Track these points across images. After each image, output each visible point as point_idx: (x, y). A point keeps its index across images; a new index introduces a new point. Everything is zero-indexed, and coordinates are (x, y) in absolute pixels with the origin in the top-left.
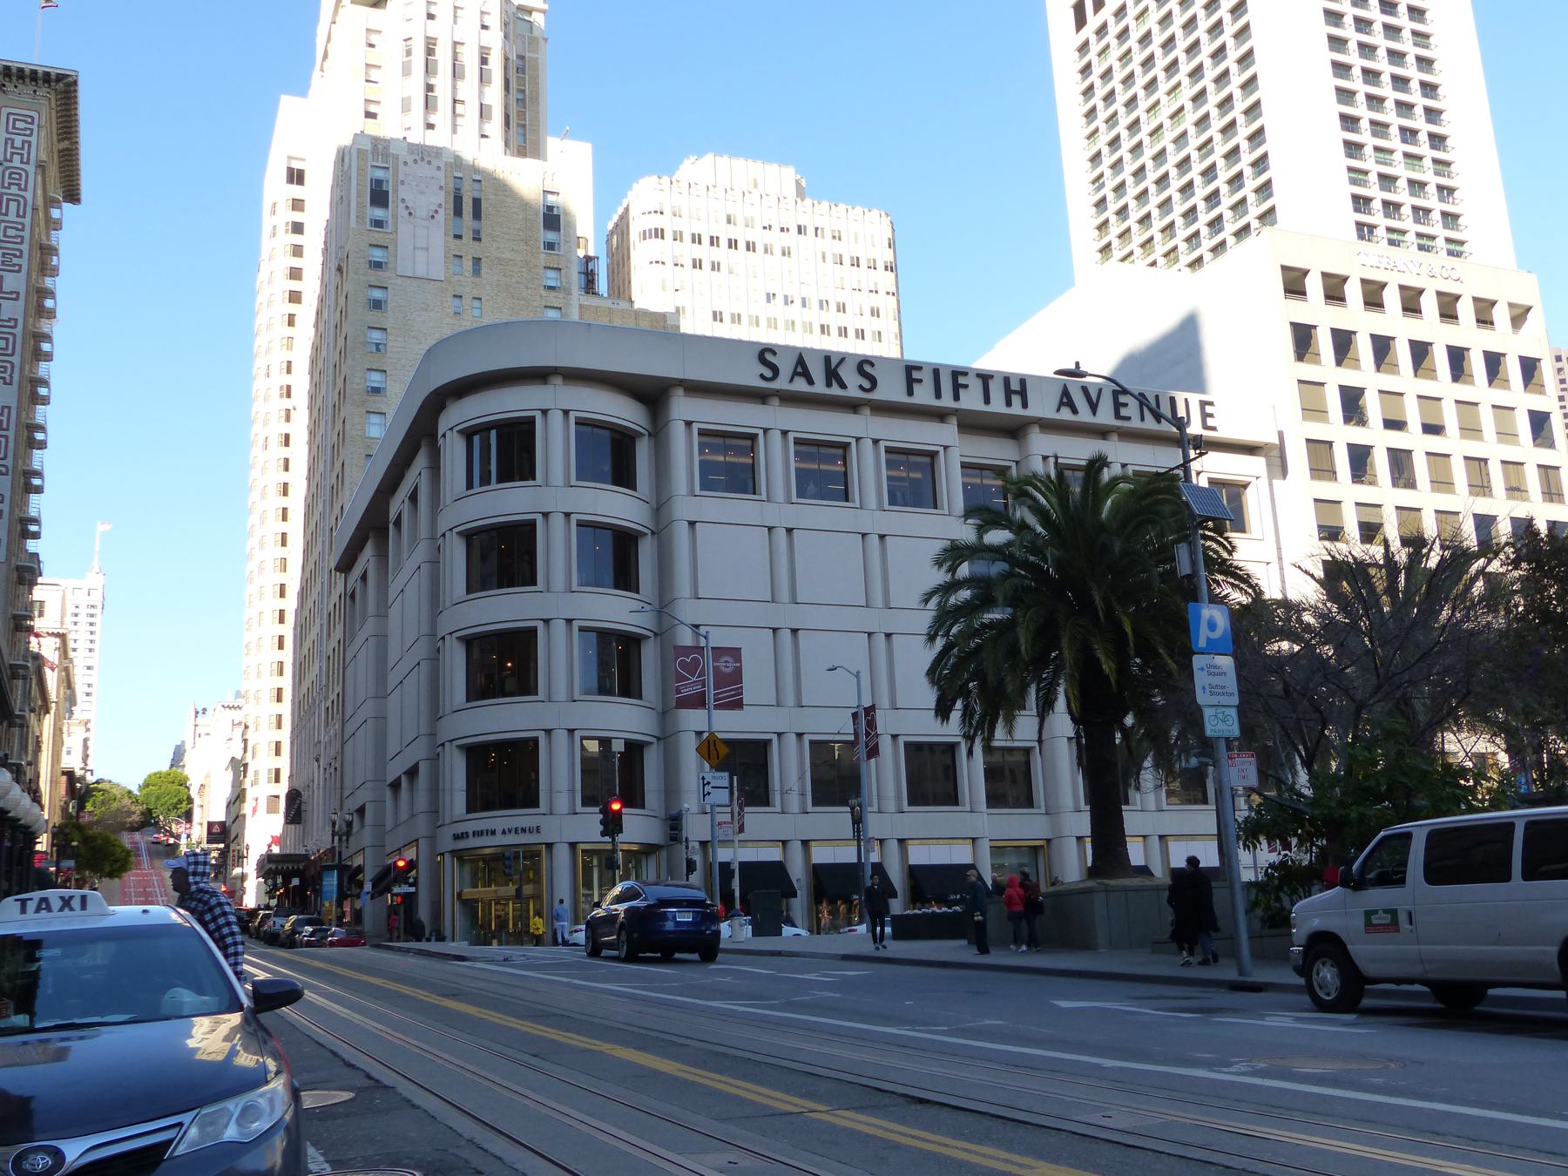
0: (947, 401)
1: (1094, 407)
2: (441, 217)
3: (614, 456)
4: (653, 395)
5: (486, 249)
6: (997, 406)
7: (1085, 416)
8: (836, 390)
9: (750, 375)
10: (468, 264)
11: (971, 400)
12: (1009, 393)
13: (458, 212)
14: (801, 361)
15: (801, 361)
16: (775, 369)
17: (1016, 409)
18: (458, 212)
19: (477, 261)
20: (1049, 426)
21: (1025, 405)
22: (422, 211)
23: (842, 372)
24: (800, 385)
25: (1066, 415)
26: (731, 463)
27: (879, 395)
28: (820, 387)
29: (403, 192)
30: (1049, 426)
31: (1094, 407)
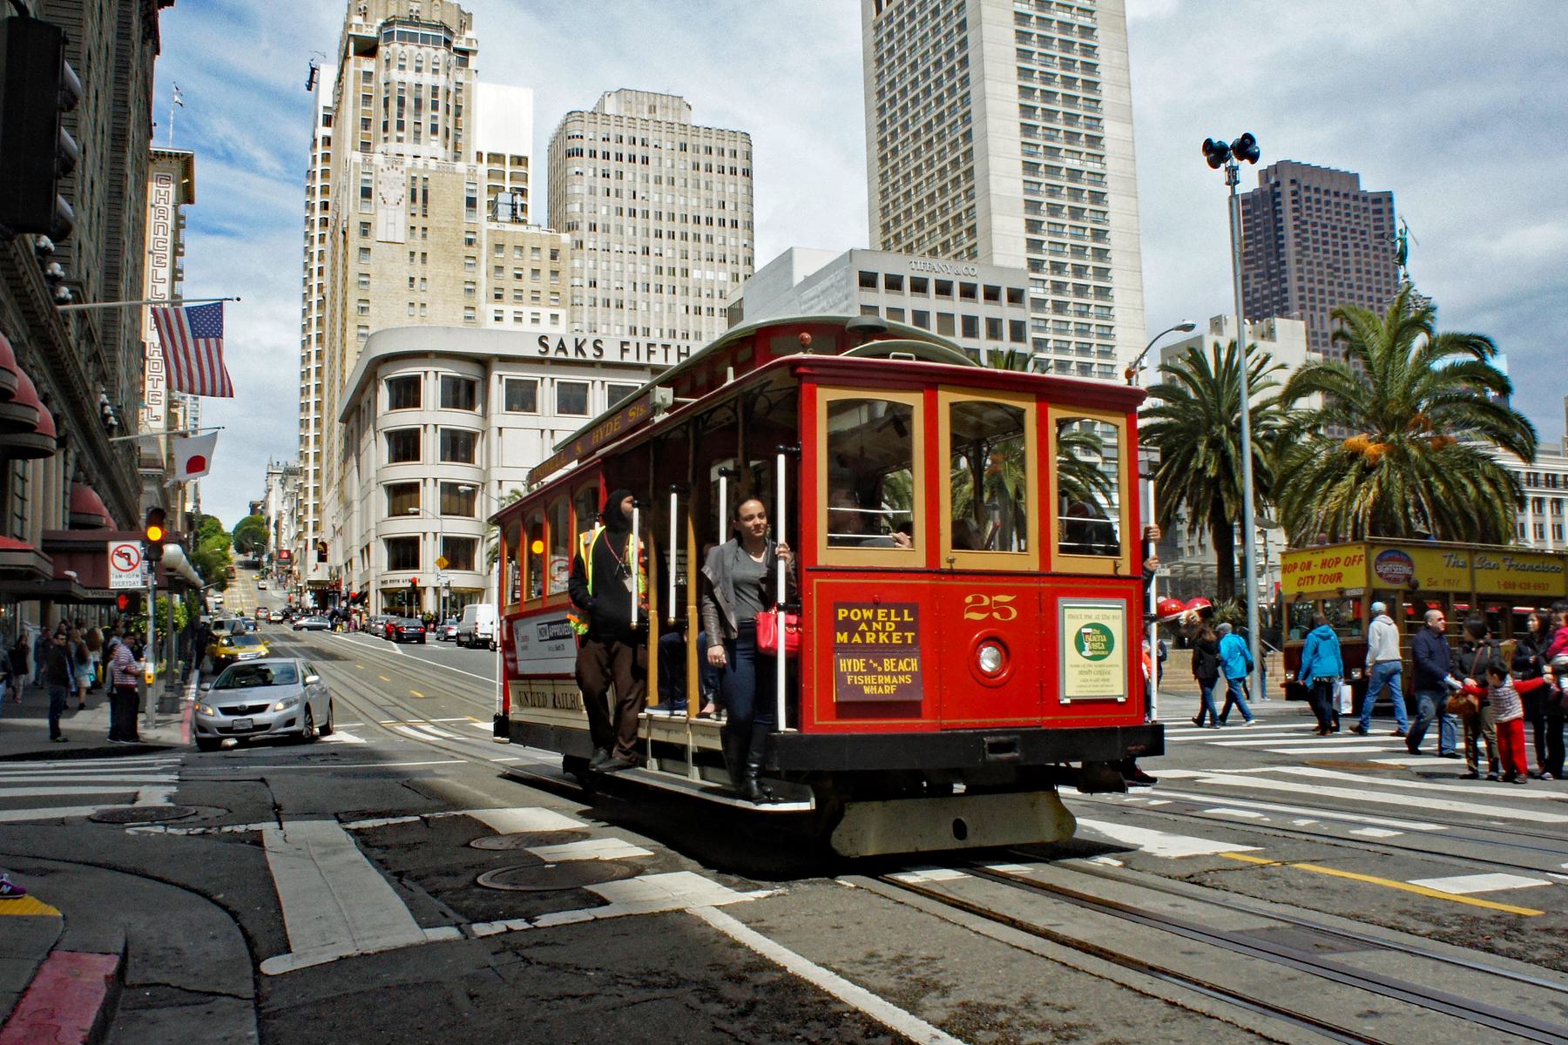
0: (643, 360)
2: (403, 204)
3: (462, 394)
4: (484, 363)
5: (430, 222)
8: (580, 357)
9: (534, 351)
10: (419, 232)
13: (414, 199)
14: (561, 342)
15: (561, 342)
16: (546, 347)
18: (414, 199)
19: (425, 229)
22: (392, 200)
24: (561, 355)
26: (521, 398)
27: (605, 358)
28: (571, 356)
29: (381, 188)
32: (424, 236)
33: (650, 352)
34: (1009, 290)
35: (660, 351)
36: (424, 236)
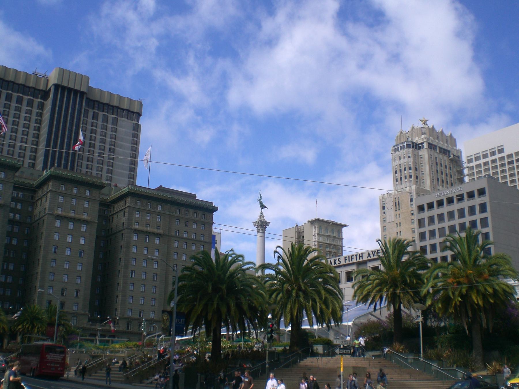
0: (351, 262)
6: (358, 260)
7: (372, 257)
10: (398, 216)
11: (354, 261)
12: (360, 257)
17: (361, 260)
20: (371, 260)
22: (390, 208)
25: (369, 258)
27: (341, 264)
30: (371, 260)
31: (374, 255)
32: (400, 217)
33: (352, 258)
34: (478, 190)
35: (354, 257)
36: (400, 217)
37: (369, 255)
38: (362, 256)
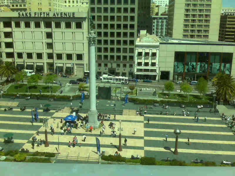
1: (58, 15)
6: (45, 16)
7: (57, 16)
11: (42, 16)
14: (23, 14)
15: (23, 14)
17: (48, 16)
21: (49, 16)
23: (27, 14)
25: (54, 16)
31: (58, 15)
37: (54, 15)
38: (49, 15)
